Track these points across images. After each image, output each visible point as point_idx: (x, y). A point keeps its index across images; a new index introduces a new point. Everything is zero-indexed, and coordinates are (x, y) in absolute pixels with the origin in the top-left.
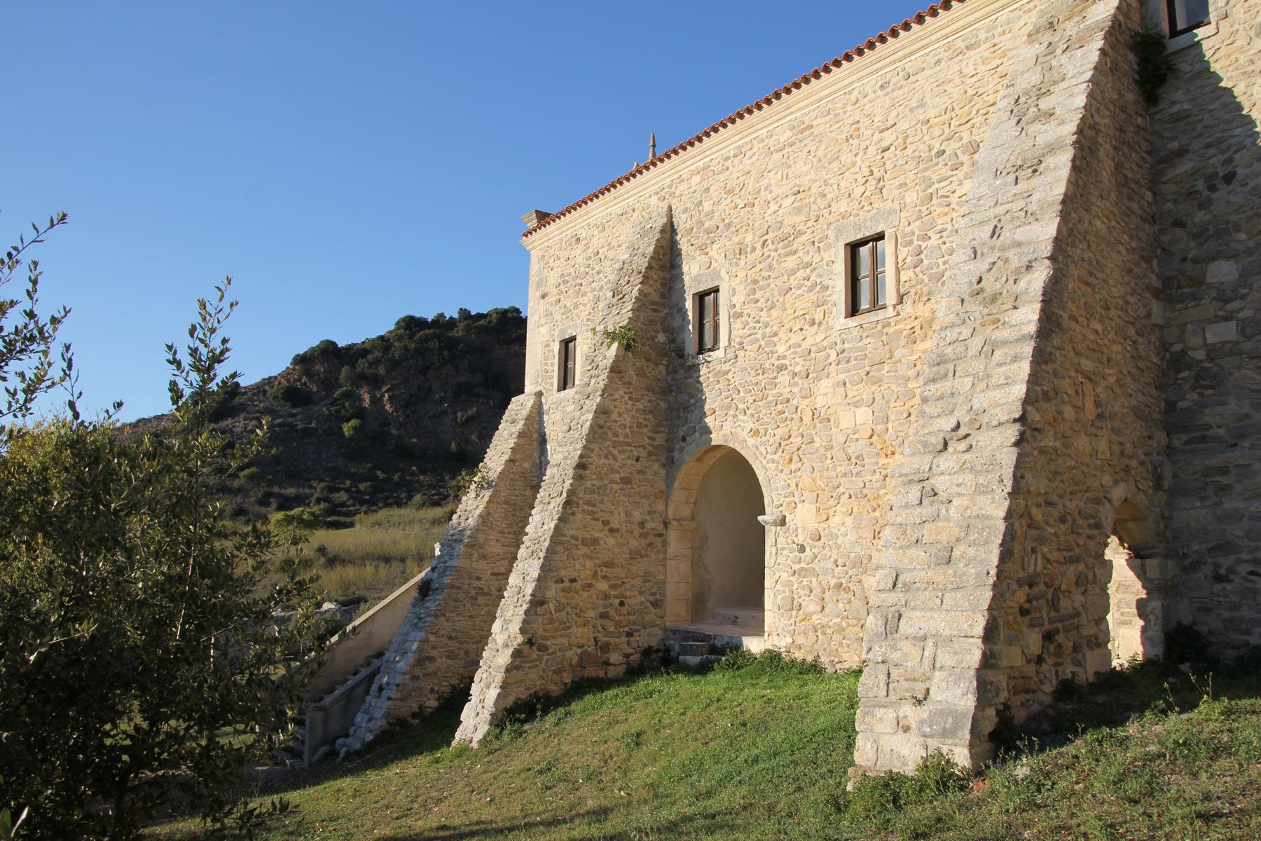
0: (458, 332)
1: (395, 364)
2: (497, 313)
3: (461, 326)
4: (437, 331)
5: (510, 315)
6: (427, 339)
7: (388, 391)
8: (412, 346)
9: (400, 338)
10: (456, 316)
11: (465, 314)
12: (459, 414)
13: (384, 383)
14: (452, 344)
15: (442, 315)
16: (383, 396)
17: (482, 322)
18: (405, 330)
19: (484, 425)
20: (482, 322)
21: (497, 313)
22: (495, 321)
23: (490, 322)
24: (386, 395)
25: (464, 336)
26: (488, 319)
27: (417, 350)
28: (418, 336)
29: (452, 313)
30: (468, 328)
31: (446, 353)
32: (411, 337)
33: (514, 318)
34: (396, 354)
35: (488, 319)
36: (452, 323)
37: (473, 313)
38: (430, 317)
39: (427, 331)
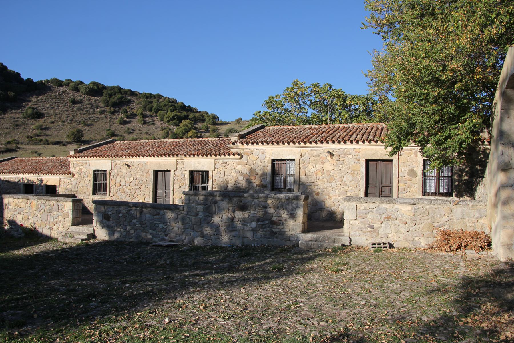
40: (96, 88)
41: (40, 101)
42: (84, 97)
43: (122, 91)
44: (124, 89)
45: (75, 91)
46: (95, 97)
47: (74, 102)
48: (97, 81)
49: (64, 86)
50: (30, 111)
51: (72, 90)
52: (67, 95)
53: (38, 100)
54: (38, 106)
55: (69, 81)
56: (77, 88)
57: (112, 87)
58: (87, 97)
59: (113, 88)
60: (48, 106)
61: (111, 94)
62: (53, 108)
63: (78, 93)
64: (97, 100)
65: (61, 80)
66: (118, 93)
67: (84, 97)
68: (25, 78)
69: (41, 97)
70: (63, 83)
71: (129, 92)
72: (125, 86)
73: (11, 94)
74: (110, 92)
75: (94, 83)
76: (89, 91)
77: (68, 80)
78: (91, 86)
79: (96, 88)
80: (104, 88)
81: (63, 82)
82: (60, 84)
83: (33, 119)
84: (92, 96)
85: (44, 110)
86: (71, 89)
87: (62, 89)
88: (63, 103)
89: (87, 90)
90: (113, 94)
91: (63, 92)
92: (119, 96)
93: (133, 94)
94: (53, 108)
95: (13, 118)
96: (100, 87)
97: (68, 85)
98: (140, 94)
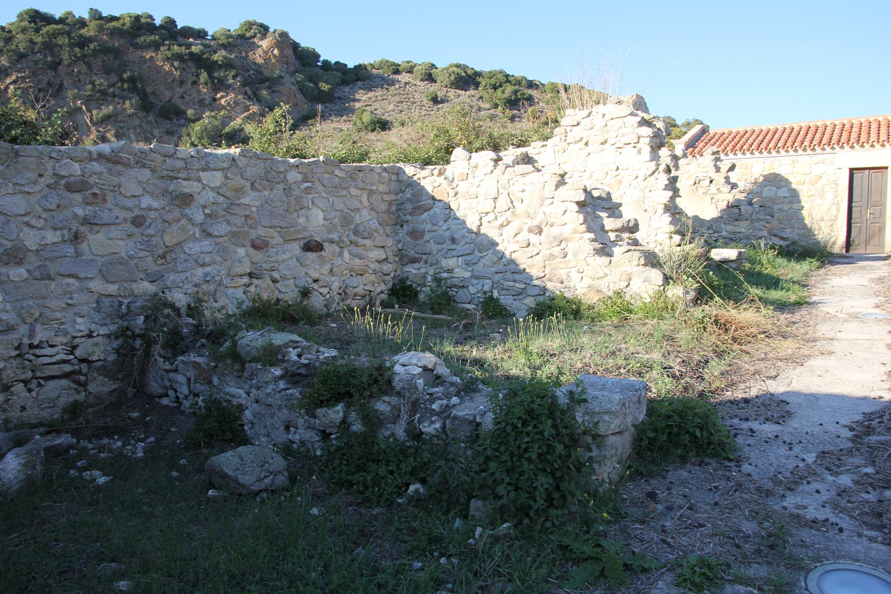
0: (89, 32)
1: (21, 56)
2: (131, 17)
3: (93, 24)
4: (67, 28)
5: (143, 20)
6: (55, 35)
7: (14, 82)
8: (38, 39)
9: (24, 30)
10: (86, 16)
11: (96, 15)
12: (94, 112)
13: (8, 75)
14: (83, 42)
15: (70, 13)
16: (7, 88)
17: (115, 24)
18: (30, 22)
19: (121, 124)
20: (115, 24)
21: (131, 17)
22: (128, 24)
23: (124, 24)
24: (12, 87)
25: (96, 36)
26: (121, 22)
27: (44, 44)
28: (45, 30)
29: (82, 12)
30: (101, 29)
31: (77, 50)
32: (37, 30)
33: (147, 24)
34: (20, 46)
35: (121, 22)
36: (82, 23)
37: (104, 15)
38: (58, 15)
39: (55, 26)
40: (463, 74)
41: (374, 99)
42: (447, 92)
43: (510, 79)
44: (513, 76)
45: (427, 80)
46: (466, 90)
47: (435, 100)
48: (462, 62)
49: (404, 73)
50: (366, 118)
51: (422, 80)
52: (414, 87)
53: (370, 98)
54: (373, 108)
55: (411, 64)
56: (430, 75)
57: (490, 72)
58: (452, 93)
59: (492, 75)
60: (391, 107)
61: (495, 85)
62: (401, 111)
63: (433, 84)
64: (473, 96)
65: (396, 62)
66: (505, 83)
67: (447, 92)
68: (333, 62)
69: (371, 94)
70: (400, 68)
71: (524, 82)
72: (515, 71)
73: (325, 87)
74: (493, 81)
75: (458, 66)
76: (455, 79)
77: (408, 62)
78: (455, 69)
79: (463, 74)
80: (478, 74)
81: (399, 65)
82: (397, 70)
83: (373, 130)
84: (462, 89)
85: (387, 114)
86: (420, 77)
87: (404, 77)
88: (415, 103)
89: (452, 78)
90: (498, 84)
91: (406, 84)
92: (509, 89)
93: (531, 85)
94: (401, 111)
95: (338, 130)
96: (469, 72)
97: (410, 71)
98: (543, 85)
